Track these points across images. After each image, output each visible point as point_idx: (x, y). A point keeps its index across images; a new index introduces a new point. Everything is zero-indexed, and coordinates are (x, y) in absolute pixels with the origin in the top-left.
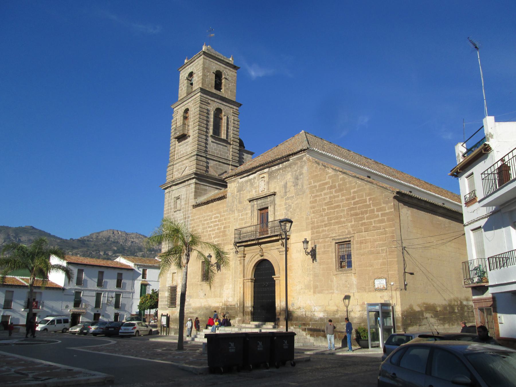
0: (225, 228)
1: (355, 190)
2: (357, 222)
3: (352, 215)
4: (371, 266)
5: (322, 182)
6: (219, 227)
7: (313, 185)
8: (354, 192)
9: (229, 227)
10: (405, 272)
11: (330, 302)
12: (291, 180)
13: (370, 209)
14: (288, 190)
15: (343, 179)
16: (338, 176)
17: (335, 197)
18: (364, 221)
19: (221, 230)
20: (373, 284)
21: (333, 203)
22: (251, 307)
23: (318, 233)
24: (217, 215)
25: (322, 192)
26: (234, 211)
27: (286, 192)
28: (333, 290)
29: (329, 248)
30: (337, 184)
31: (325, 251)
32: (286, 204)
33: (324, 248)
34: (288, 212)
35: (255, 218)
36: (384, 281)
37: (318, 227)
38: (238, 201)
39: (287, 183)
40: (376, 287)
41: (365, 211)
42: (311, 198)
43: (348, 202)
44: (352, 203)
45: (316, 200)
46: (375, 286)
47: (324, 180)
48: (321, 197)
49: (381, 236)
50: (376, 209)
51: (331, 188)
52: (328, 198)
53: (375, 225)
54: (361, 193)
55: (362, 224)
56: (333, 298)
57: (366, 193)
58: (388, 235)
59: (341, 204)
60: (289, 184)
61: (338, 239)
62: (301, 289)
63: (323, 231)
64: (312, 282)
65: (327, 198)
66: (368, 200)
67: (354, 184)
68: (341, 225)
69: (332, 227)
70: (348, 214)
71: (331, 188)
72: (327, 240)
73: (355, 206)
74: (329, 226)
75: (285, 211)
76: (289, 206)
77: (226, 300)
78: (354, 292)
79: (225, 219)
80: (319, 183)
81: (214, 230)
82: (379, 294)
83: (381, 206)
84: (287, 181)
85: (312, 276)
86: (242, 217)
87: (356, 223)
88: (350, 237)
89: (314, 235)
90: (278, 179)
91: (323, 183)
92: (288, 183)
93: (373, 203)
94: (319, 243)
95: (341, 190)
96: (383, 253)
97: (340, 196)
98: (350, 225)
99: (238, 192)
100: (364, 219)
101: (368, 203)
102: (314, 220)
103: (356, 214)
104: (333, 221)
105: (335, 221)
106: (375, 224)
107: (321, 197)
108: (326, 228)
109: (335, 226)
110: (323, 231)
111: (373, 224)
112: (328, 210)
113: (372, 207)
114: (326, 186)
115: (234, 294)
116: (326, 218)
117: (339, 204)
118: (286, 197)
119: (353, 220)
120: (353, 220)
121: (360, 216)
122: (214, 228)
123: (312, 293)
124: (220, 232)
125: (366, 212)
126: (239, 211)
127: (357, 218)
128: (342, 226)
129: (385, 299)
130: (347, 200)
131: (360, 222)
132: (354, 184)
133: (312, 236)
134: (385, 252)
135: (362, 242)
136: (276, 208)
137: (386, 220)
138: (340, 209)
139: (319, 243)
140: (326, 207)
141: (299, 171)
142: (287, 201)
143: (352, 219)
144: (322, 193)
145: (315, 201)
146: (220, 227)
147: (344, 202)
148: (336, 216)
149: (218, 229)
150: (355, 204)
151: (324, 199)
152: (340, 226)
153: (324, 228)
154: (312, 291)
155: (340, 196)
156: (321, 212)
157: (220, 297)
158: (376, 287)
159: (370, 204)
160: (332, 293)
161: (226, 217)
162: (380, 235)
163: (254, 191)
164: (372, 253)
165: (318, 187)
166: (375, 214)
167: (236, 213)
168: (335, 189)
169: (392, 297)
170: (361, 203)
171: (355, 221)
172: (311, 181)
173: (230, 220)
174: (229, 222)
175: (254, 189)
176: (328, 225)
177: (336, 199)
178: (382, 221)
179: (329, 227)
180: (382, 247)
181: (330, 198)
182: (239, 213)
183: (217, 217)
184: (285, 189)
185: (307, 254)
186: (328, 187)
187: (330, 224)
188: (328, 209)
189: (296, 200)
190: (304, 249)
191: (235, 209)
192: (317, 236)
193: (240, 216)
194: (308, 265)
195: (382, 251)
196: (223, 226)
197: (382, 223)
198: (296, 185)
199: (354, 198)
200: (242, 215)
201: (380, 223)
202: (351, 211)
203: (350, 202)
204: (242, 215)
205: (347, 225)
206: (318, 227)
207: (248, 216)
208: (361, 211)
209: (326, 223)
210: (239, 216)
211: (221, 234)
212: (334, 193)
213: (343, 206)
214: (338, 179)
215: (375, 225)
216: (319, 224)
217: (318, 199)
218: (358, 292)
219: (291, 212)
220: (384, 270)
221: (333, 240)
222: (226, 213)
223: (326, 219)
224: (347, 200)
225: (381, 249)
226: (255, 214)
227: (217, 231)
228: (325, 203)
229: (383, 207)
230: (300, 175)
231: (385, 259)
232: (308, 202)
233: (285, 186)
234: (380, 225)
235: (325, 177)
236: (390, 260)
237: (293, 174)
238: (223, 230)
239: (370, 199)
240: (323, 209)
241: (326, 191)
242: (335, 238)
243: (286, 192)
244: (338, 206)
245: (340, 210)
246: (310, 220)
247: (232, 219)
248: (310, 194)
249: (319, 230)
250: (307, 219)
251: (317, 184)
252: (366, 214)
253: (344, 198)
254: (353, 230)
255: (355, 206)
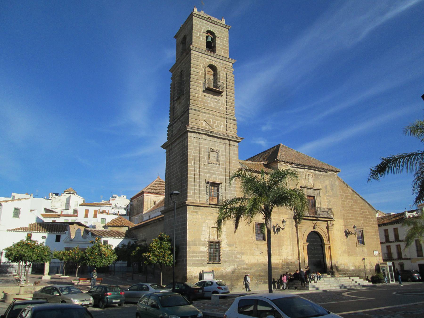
4: (371, 244)
8: (362, 206)
39: (326, 186)
62: (341, 253)
63: (350, 222)
64: (347, 249)
77: (285, 258)
100: (367, 221)
108: (351, 221)
110: (350, 222)
115: (293, 254)
128: (358, 222)
154: (347, 254)
160: (357, 256)
187: (353, 219)
194: (344, 240)
218: (368, 256)
244: (355, 211)
250: (341, 212)
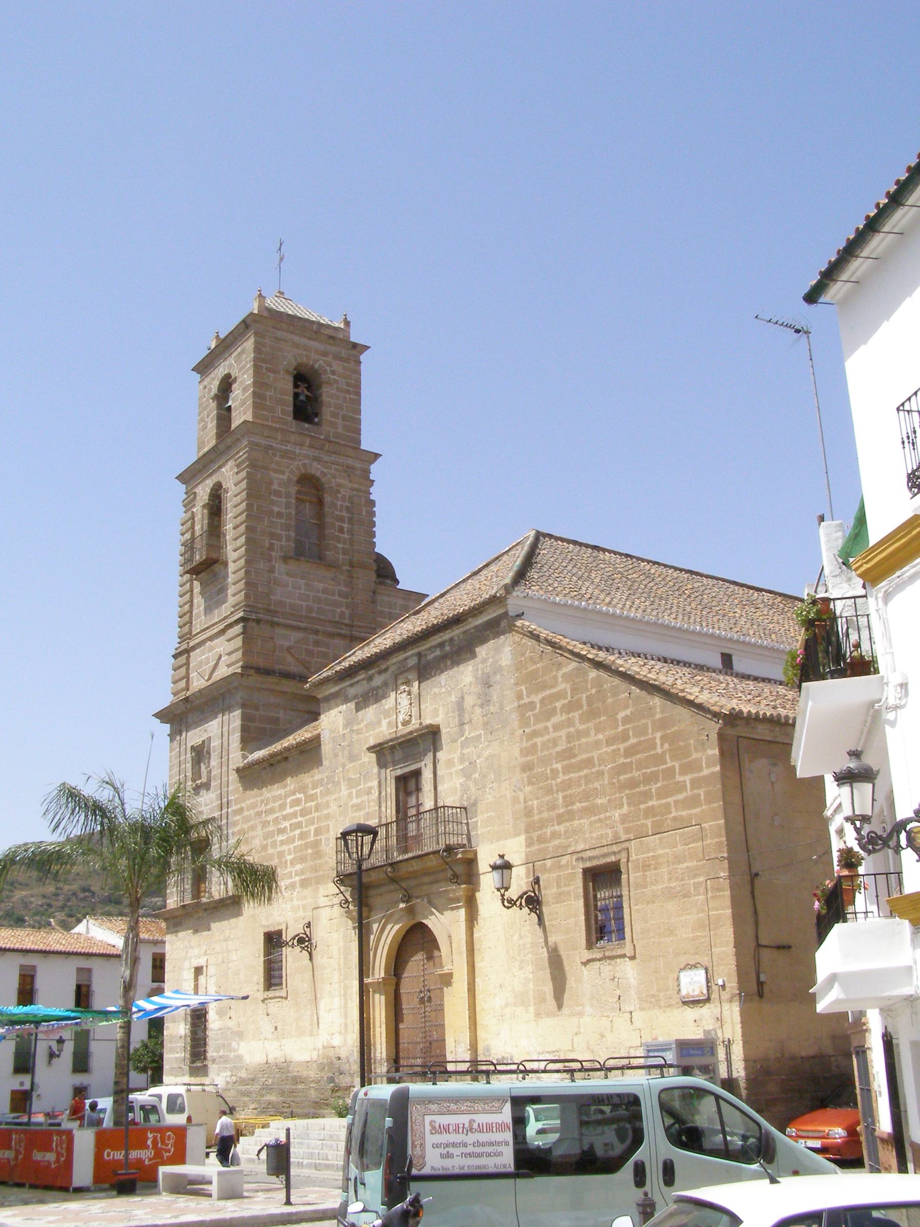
0: (317, 832)
1: (628, 712)
2: (634, 806)
3: (622, 787)
4: (671, 932)
5: (548, 692)
6: (304, 829)
7: (526, 700)
8: (626, 720)
9: (328, 831)
10: (759, 946)
11: (576, 1039)
12: (474, 689)
13: (664, 767)
14: (467, 717)
15: (598, 683)
16: (586, 674)
17: (580, 734)
18: (650, 803)
19: (308, 840)
20: (676, 984)
21: (576, 752)
22: (388, 1061)
23: (543, 843)
24: (298, 796)
25: (549, 720)
26: (339, 782)
27: (462, 724)
28: (583, 1005)
29: (569, 885)
30: (584, 696)
31: (560, 894)
32: (462, 759)
33: (559, 886)
34: (468, 783)
35: (389, 803)
36: (699, 976)
37: (543, 824)
38: (346, 752)
39: (463, 698)
40: (684, 992)
41: (652, 772)
42: (522, 739)
43: (612, 748)
44: (622, 750)
45: (535, 745)
46: (679, 990)
47: (552, 687)
48: (547, 737)
49: (692, 845)
50: (680, 766)
51: (570, 707)
52: (564, 738)
53: (679, 813)
54: (643, 721)
55: (649, 812)
56: (582, 1030)
57: (653, 723)
58: (709, 841)
59: (595, 754)
60: (470, 701)
61: (590, 859)
62: (507, 1005)
63: (555, 835)
64: (531, 986)
65: (561, 737)
66: (658, 741)
67: (623, 696)
68: (597, 818)
69: (576, 823)
70: (614, 783)
71: (570, 707)
72: (564, 860)
73: (629, 760)
74: (567, 821)
75: (462, 780)
76: (470, 763)
77: (325, 1042)
78: (632, 1009)
79: (317, 809)
80: (540, 696)
81: (291, 840)
82: (691, 1013)
83: (690, 759)
84: (464, 691)
85: (530, 968)
86: (359, 801)
87: (632, 808)
88: (620, 852)
89: (532, 849)
90: (442, 686)
91: (550, 696)
92: (466, 697)
93: (670, 751)
94: (545, 870)
95: (592, 714)
96: (699, 894)
97: (593, 732)
98: (617, 815)
99: (346, 726)
100: (651, 798)
101: (659, 751)
102: (533, 804)
103: (633, 784)
104: (577, 806)
105: (583, 804)
106: (677, 811)
107: (547, 737)
108: (561, 828)
109: (582, 821)
110: (555, 835)
111: (673, 810)
112: (564, 773)
113: (668, 761)
114: (558, 704)
115: (346, 1025)
116: (560, 795)
117: (591, 755)
118: (463, 738)
119: (624, 799)
120: (624, 799)
121: (642, 788)
122: (292, 834)
123: (533, 1015)
124: (307, 846)
125: (652, 778)
126: (351, 783)
127: (633, 794)
128: (600, 820)
129: (706, 1028)
130: (609, 742)
131: (642, 806)
132: (623, 696)
133: (528, 850)
134: (702, 890)
135: (647, 863)
136: (439, 773)
137: (702, 797)
138: (594, 770)
139: (545, 870)
140: (559, 766)
141: (491, 660)
142: (465, 751)
143: (622, 797)
144: (549, 724)
145: (532, 750)
146: (307, 829)
147: (602, 749)
148: (584, 790)
149: (302, 836)
150: (628, 753)
151: (555, 742)
152: (593, 819)
153: (557, 828)
154: (532, 1009)
155: (593, 732)
156: (547, 779)
157: (312, 1035)
158: (684, 992)
159: (664, 753)
160: (581, 1014)
161: (320, 801)
162: (689, 844)
163: (384, 722)
164: (670, 894)
165: (538, 706)
166: (678, 782)
167: (343, 788)
168: (580, 712)
169: (720, 1019)
170: (642, 751)
171: (629, 805)
172: (521, 690)
173: (329, 810)
174: (327, 817)
175: (385, 718)
176: (566, 818)
177: (584, 740)
178: (693, 801)
179: (568, 824)
180: (695, 876)
181: (569, 737)
182: (350, 787)
183: (297, 802)
184: (460, 715)
185: (506, 904)
186: (563, 705)
187: (569, 816)
188: (566, 770)
189: (488, 746)
190: (498, 890)
191: (341, 775)
192: (539, 850)
193: (352, 798)
194: (521, 937)
195: (695, 888)
196: (312, 828)
197: (695, 807)
198: (485, 701)
199: (625, 737)
200: (358, 796)
201: (689, 808)
202: (619, 774)
203: (615, 747)
204: (358, 796)
205: (611, 817)
206: (543, 824)
207: (372, 797)
208: (644, 774)
209: (562, 811)
210: (350, 796)
211: (310, 851)
212: (577, 722)
213: (602, 761)
214: (586, 681)
215: (679, 813)
216: (545, 815)
217: (539, 740)
218: (642, 1009)
219: (476, 782)
220: (702, 942)
221: (577, 860)
222: (318, 790)
223: (561, 801)
224: (609, 742)
225: (692, 881)
226: (389, 790)
227: (300, 842)
228: (557, 753)
229: (696, 760)
230: (495, 673)
231: (704, 911)
232: (516, 752)
233: (460, 707)
234: (690, 812)
235: (555, 678)
236: (715, 913)
237: (477, 670)
238: (312, 838)
239: (664, 739)
240: (552, 771)
241: (556, 719)
242: (584, 855)
243: (462, 724)
244: (589, 762)
245: (592, 773)
246: (522, 806)
247: (334, 808)
248: (521, 728)
249: (545, 833)
250: (515, 800)
251: (536, 698)
252: (655, 783)
253: (600, 736)
254: (627, 831)
255: (629, 760)
